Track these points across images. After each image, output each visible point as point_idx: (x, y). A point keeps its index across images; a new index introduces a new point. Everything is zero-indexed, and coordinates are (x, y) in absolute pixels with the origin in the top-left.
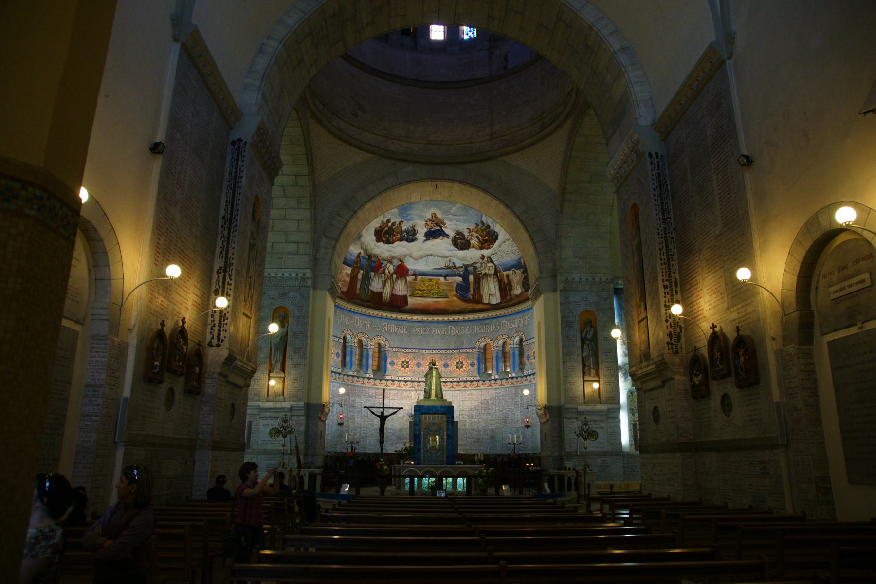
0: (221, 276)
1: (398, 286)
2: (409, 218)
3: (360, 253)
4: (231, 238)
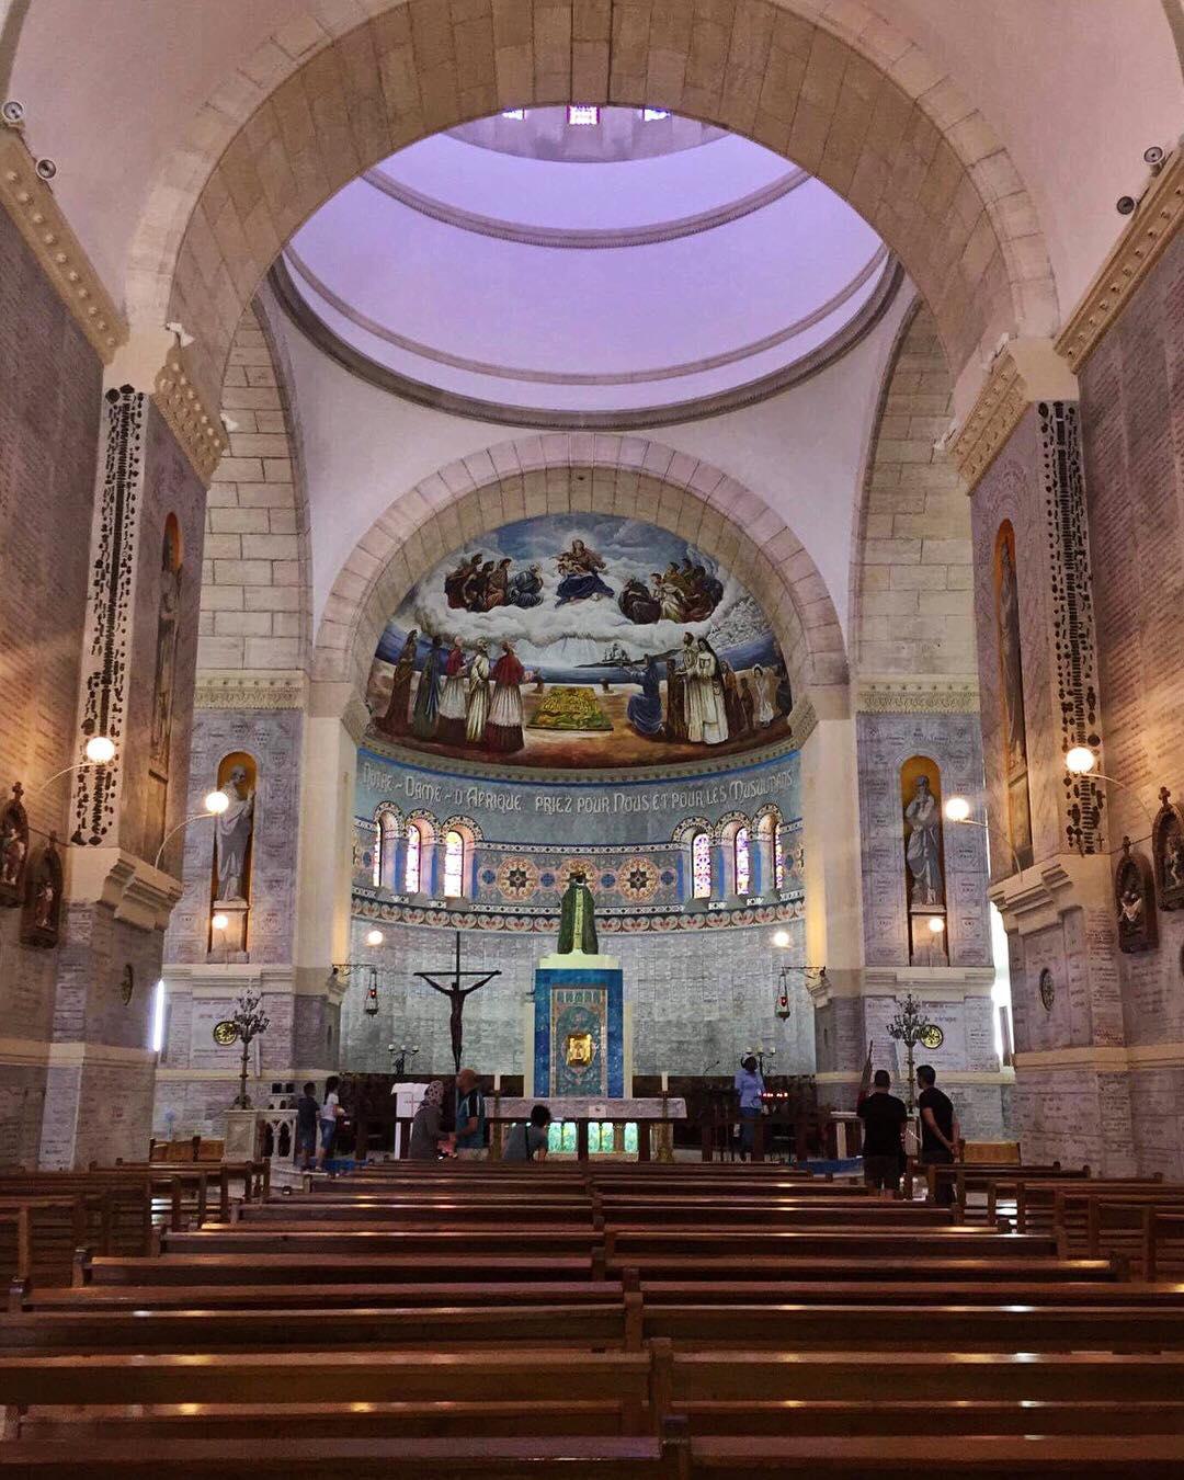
0: (99, 690)
3: (414, 632)
4: (117, 610)
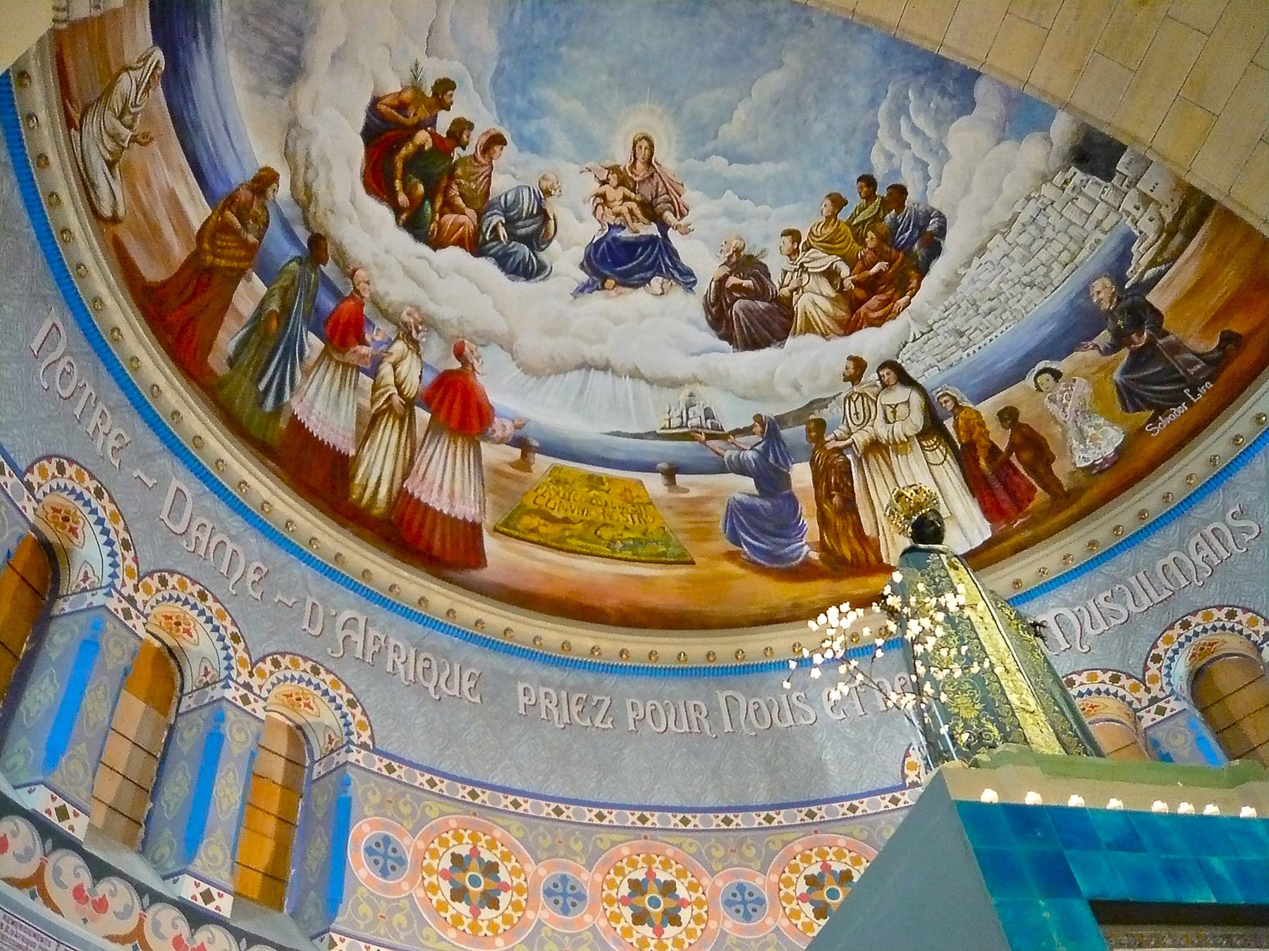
1: (436, 469)
2: (530, 129)
